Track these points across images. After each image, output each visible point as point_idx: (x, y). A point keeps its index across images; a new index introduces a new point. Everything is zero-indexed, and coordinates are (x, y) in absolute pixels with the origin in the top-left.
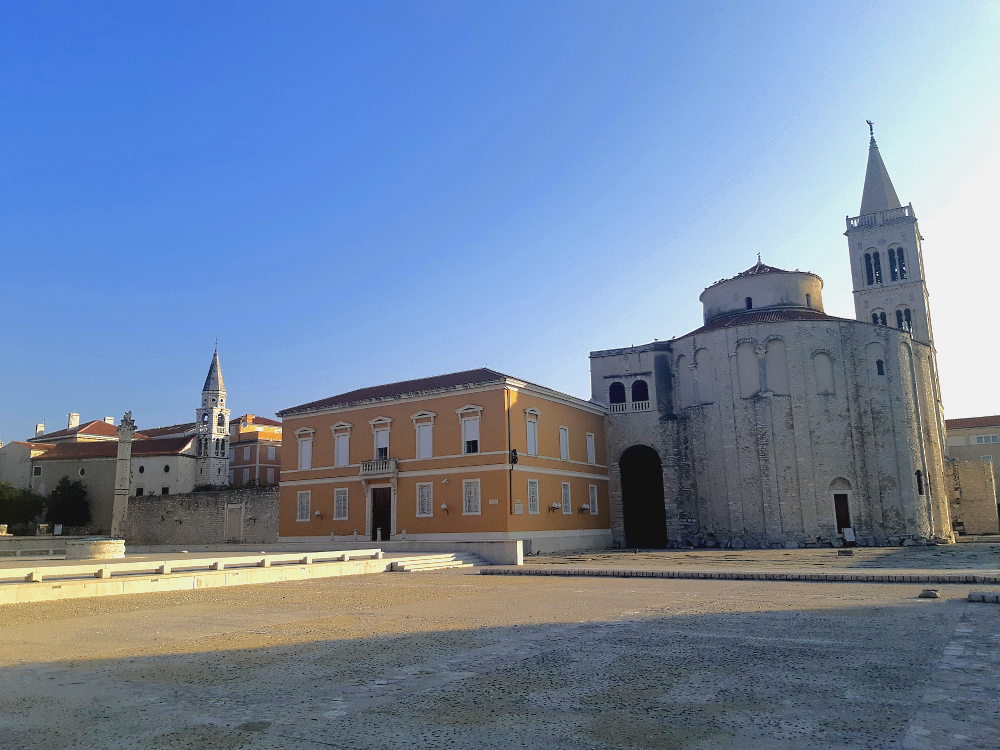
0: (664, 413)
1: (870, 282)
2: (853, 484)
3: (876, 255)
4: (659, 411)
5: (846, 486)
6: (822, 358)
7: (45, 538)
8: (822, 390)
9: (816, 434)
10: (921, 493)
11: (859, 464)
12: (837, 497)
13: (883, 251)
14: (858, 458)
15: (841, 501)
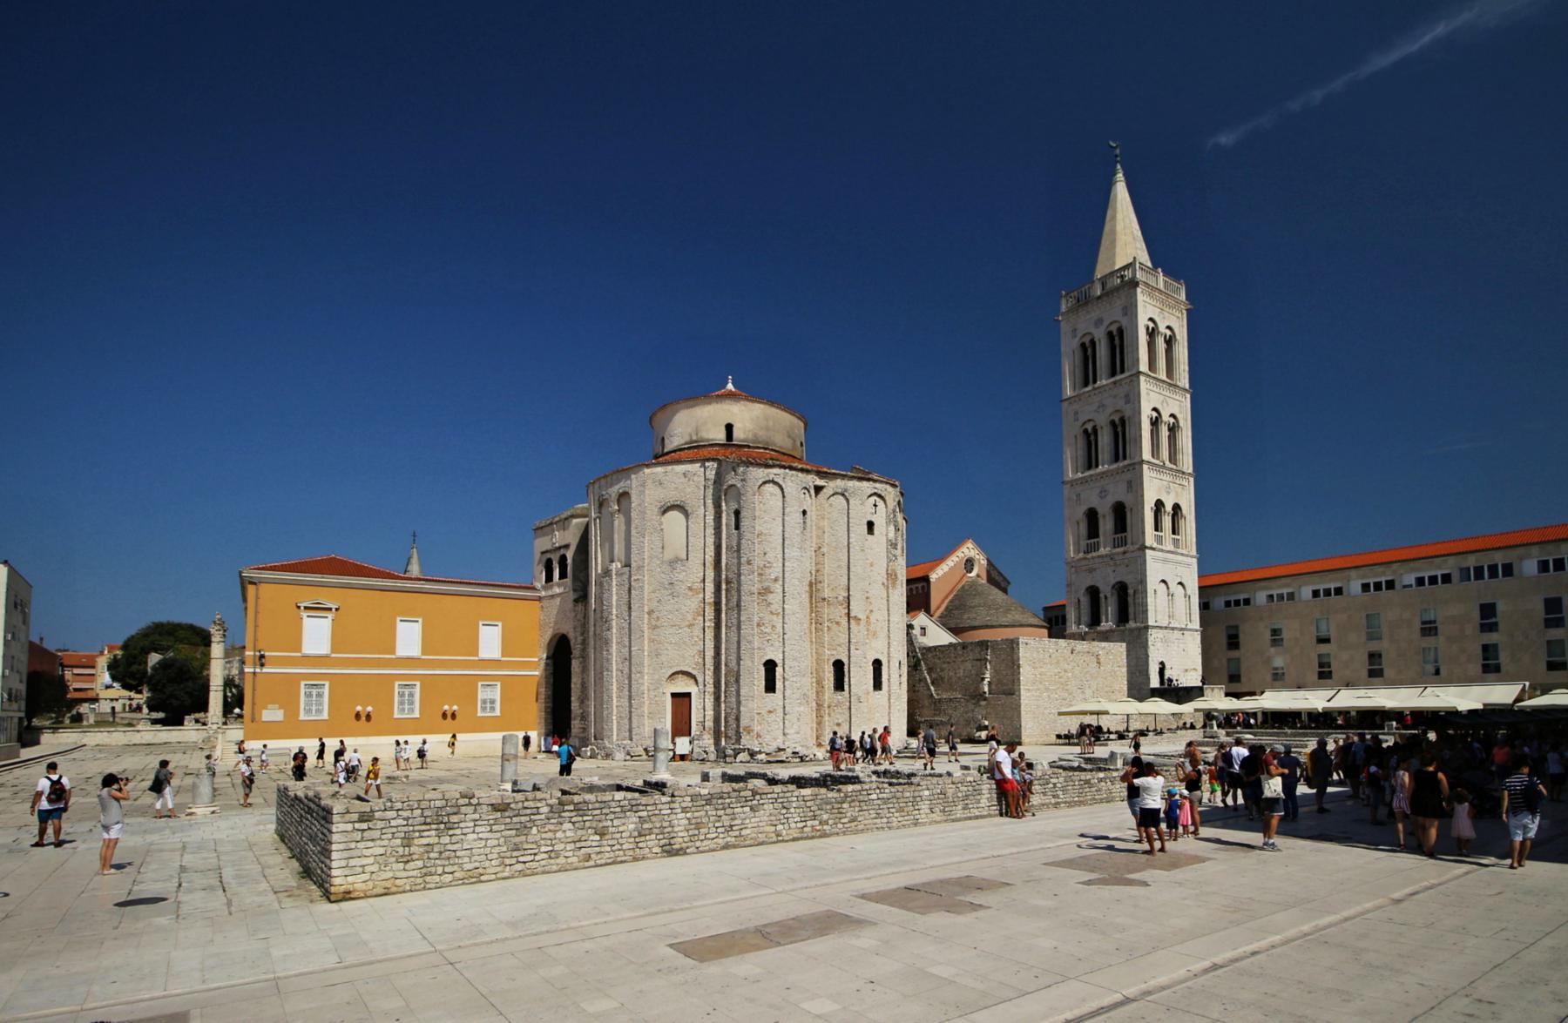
0: (581, 593)
1: (1086, 384)
2: (700, 679)
3: (1093, 343)
4: (574, 590)
5: (692, 681)
6: (674, 515)
7: (235, 727)
8: (669, 555)
9: (654, 616)
10: (877, 685)
11: (710, 653)
12: (674, 695)
13: (1100, 335)
14: (710, 645)
15: (681, 699)
